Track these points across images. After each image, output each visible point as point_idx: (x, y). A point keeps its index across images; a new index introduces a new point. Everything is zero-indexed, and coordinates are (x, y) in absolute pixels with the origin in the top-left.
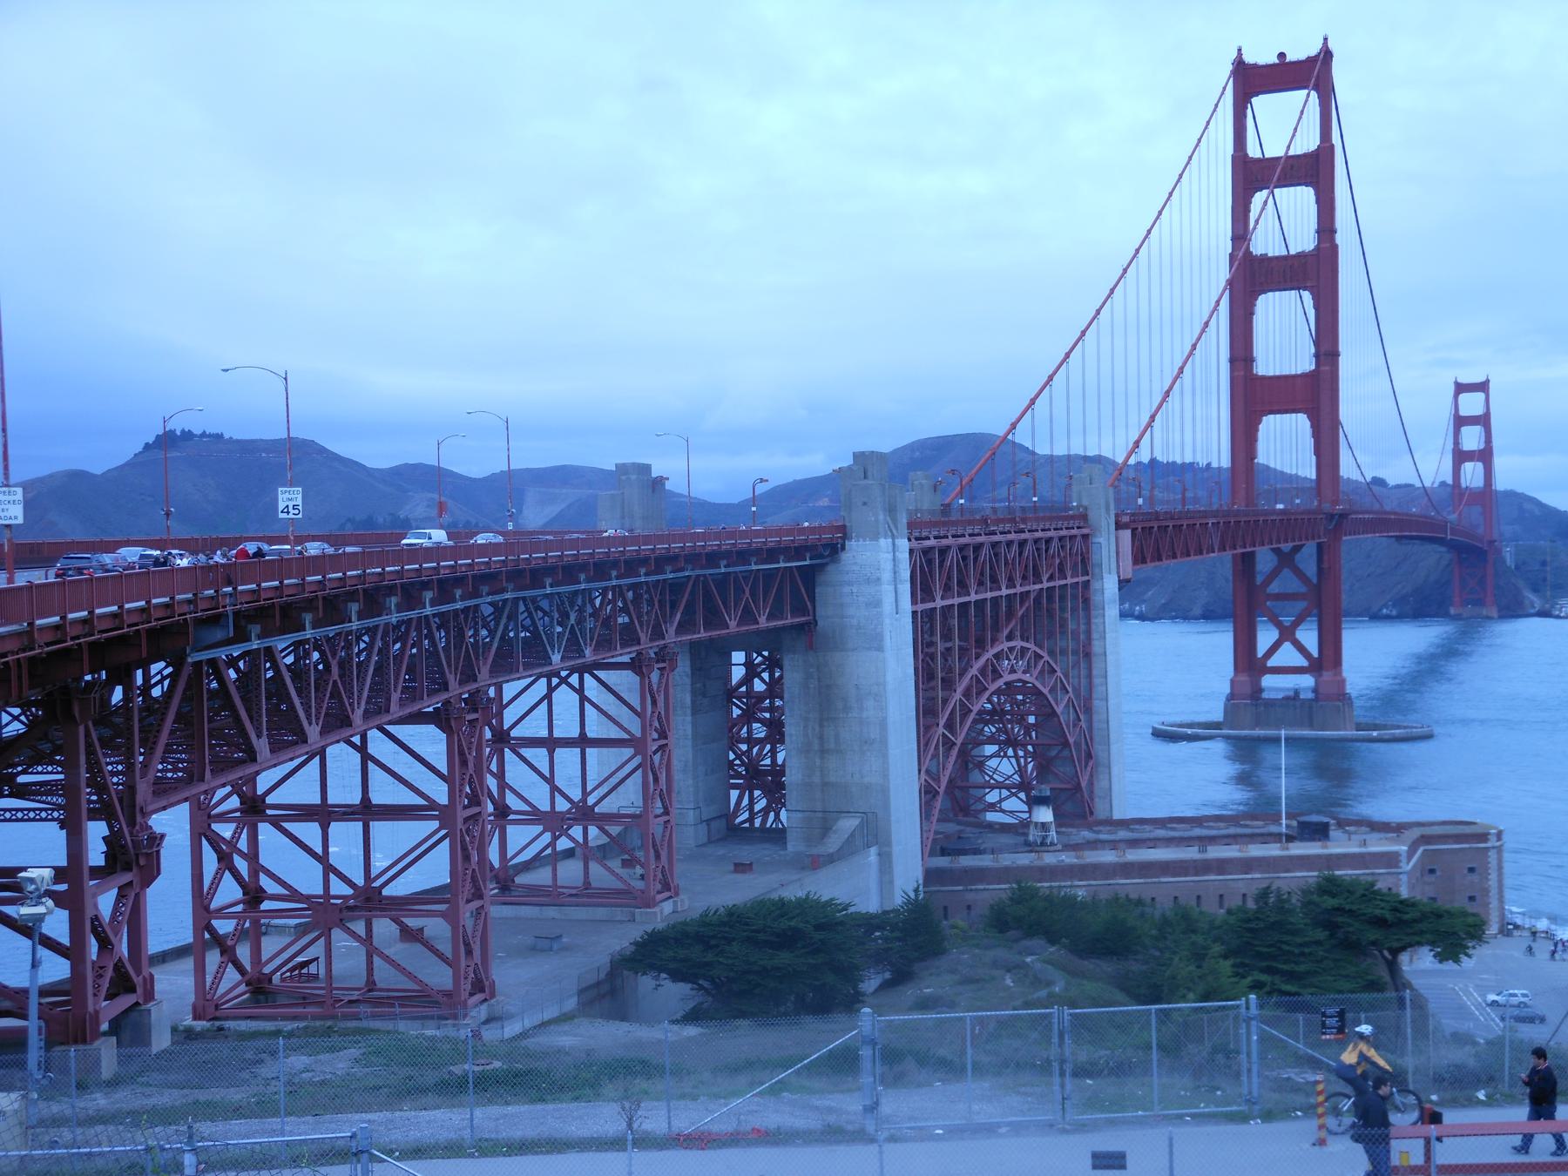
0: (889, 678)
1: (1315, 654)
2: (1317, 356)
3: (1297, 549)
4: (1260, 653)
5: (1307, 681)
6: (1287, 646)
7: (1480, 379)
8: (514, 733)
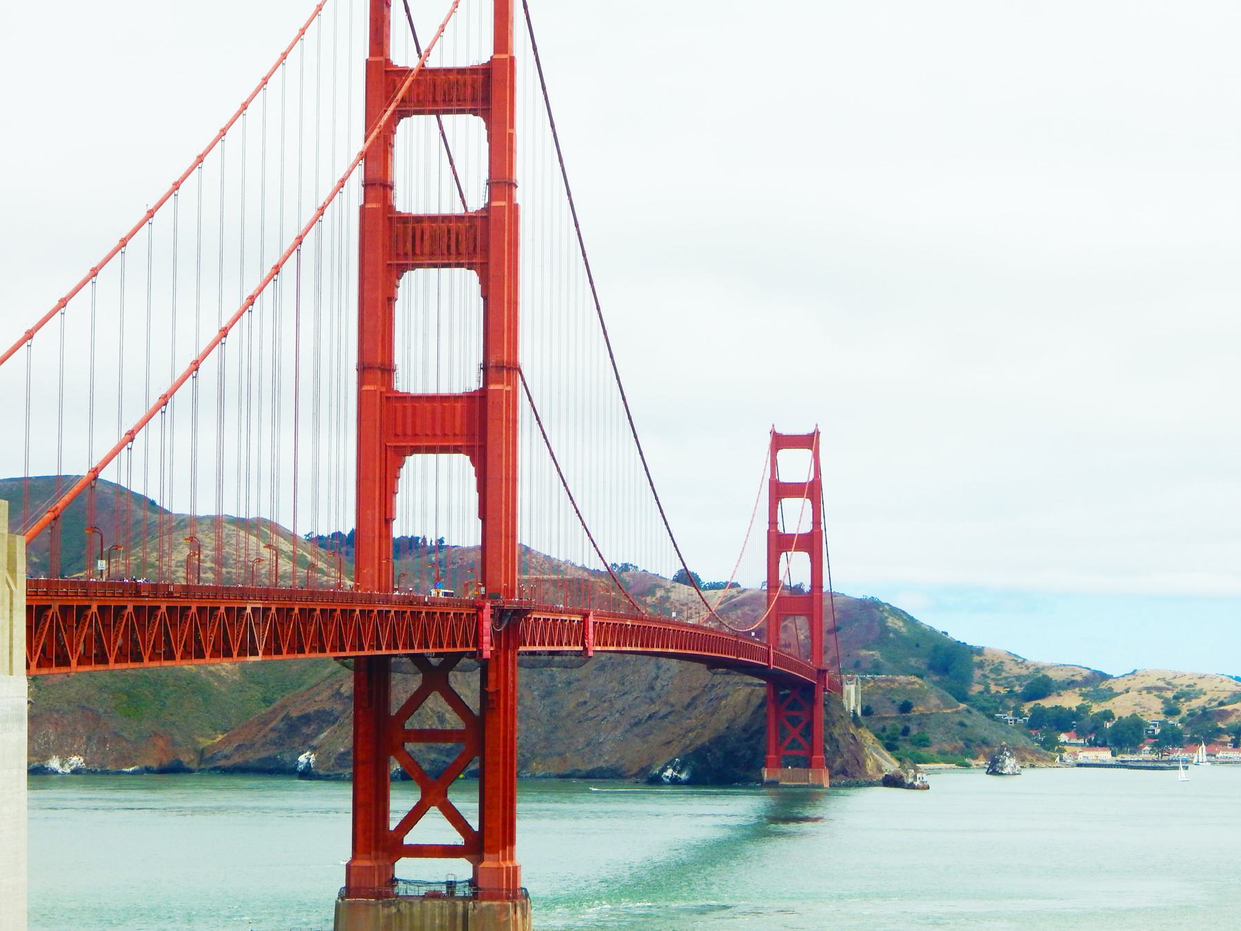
1: (475, 825)
2: (485, 368)
3: (451, 661)
4: (393, 825)
5: (461, 869)
6: (434, 810)
7: (804, 430)
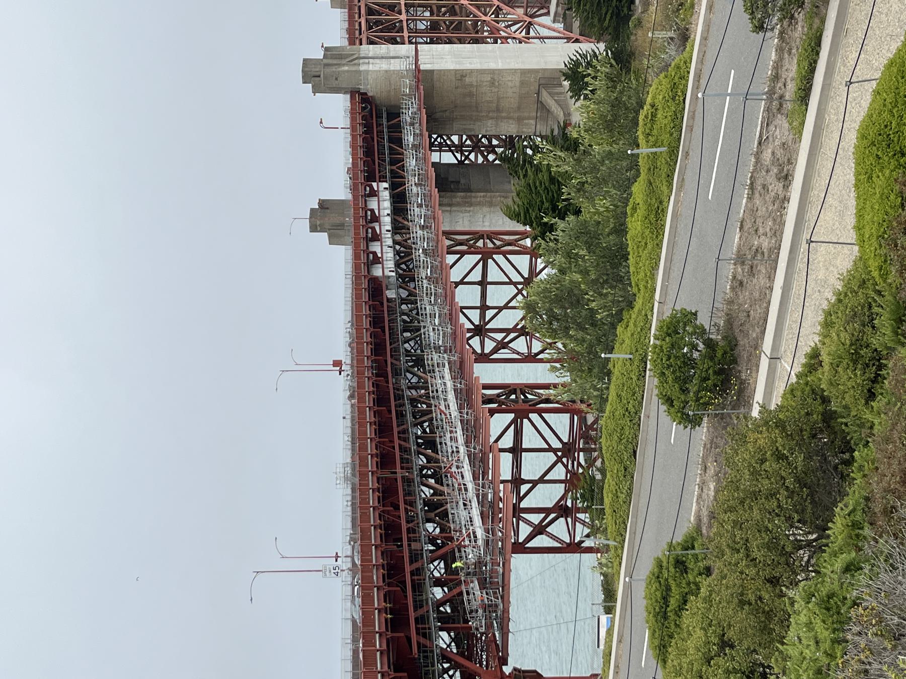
0: (451, 66)
8: (477, 323)
